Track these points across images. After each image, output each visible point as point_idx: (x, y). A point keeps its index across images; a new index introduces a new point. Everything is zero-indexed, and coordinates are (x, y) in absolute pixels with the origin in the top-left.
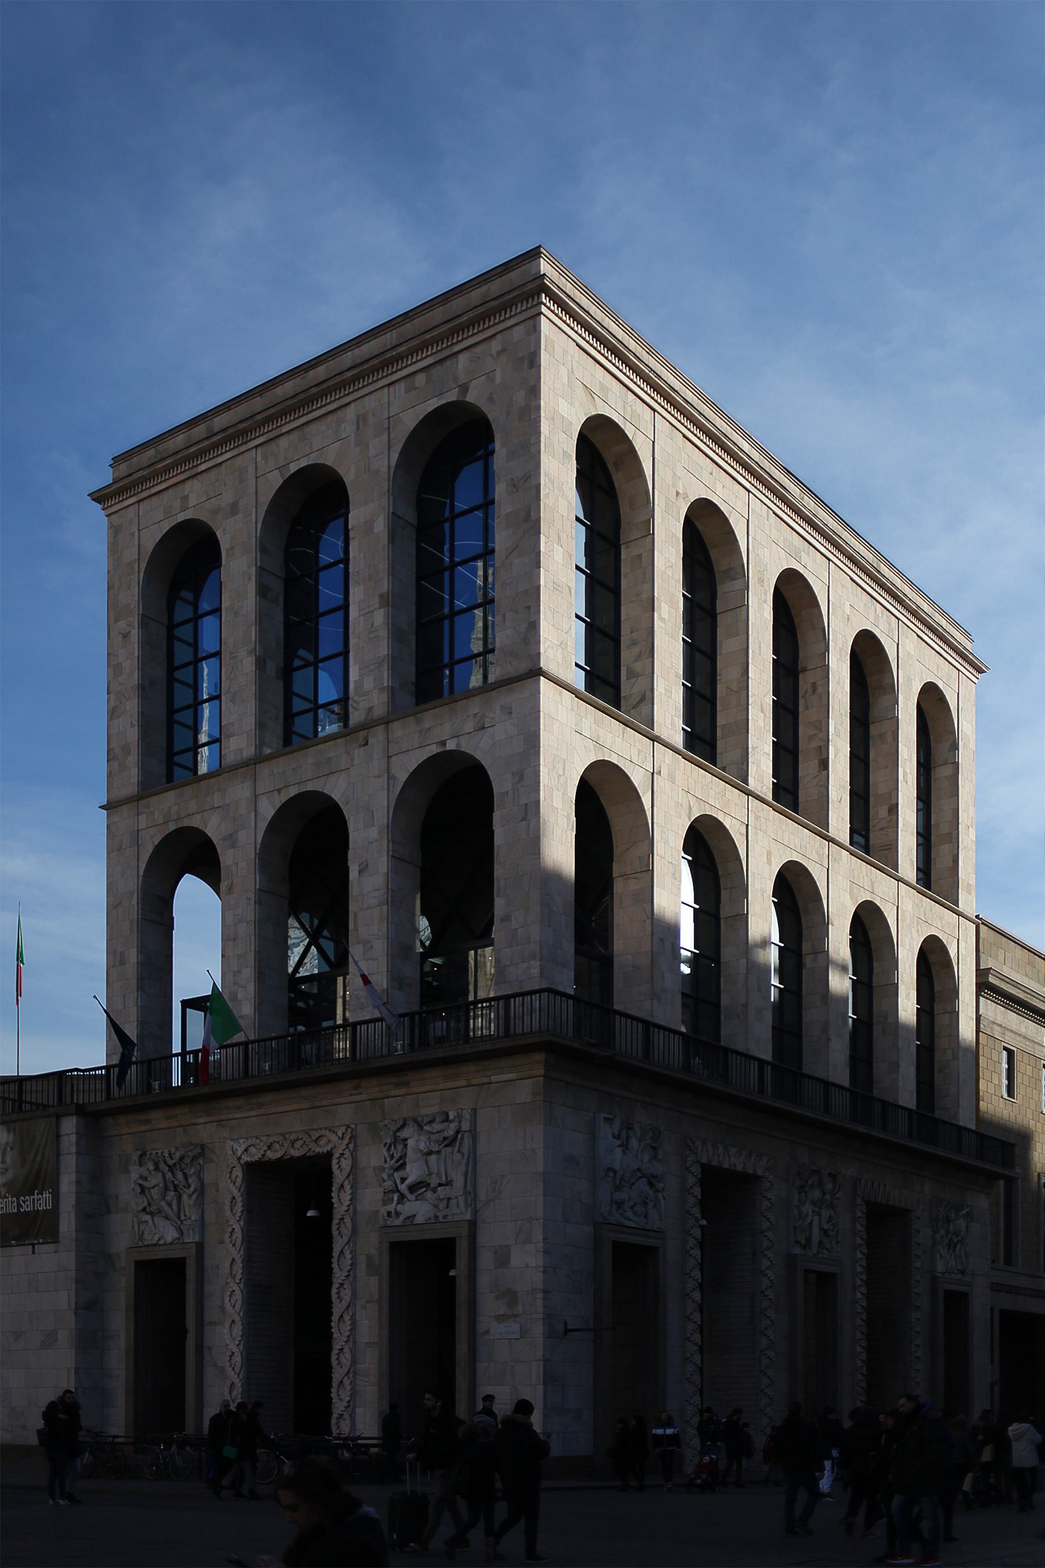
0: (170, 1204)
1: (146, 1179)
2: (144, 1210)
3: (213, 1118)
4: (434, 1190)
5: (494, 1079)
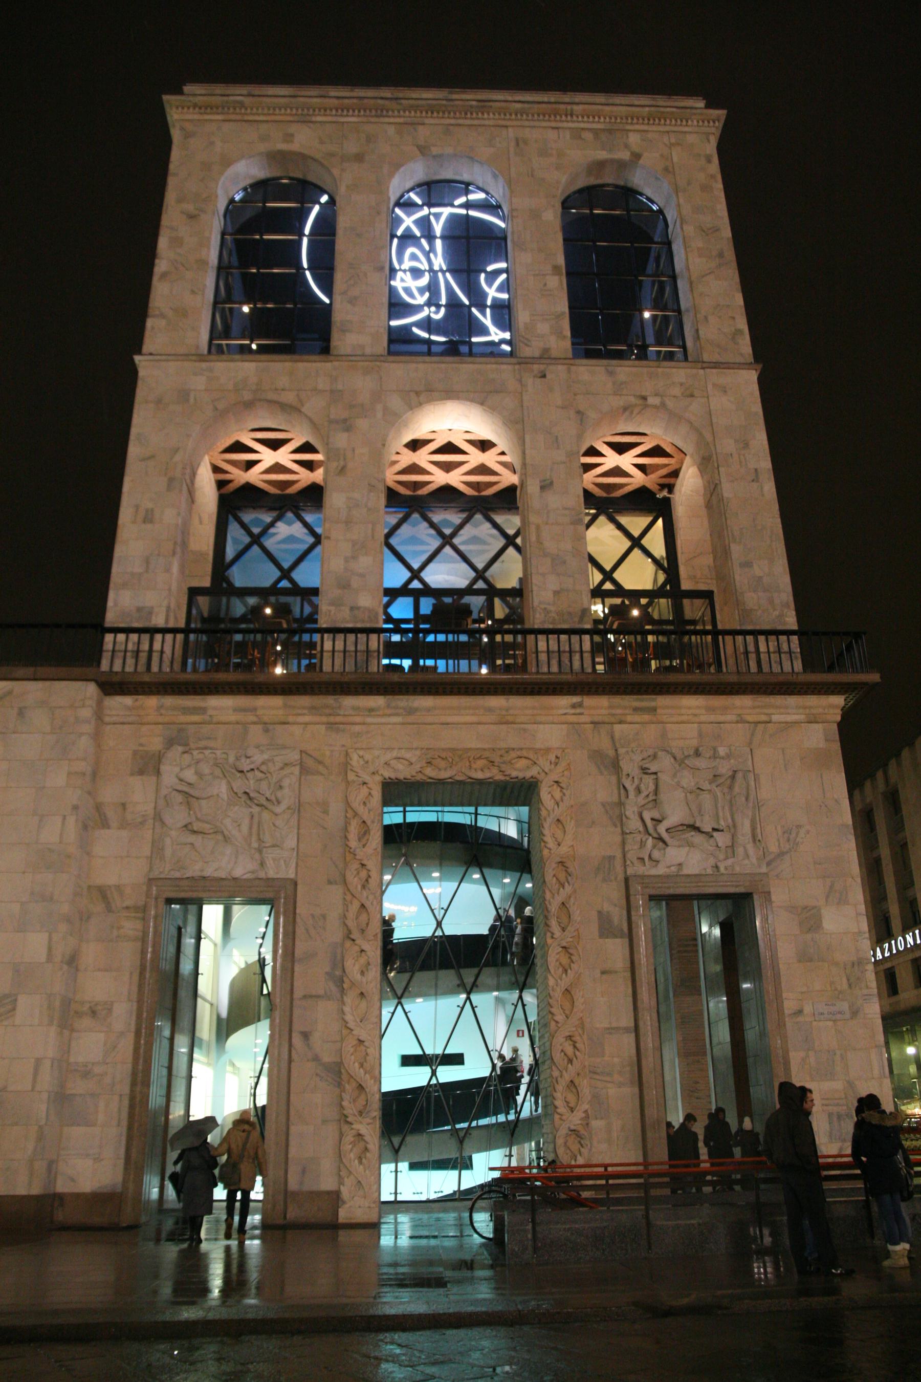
5: (775, 718)
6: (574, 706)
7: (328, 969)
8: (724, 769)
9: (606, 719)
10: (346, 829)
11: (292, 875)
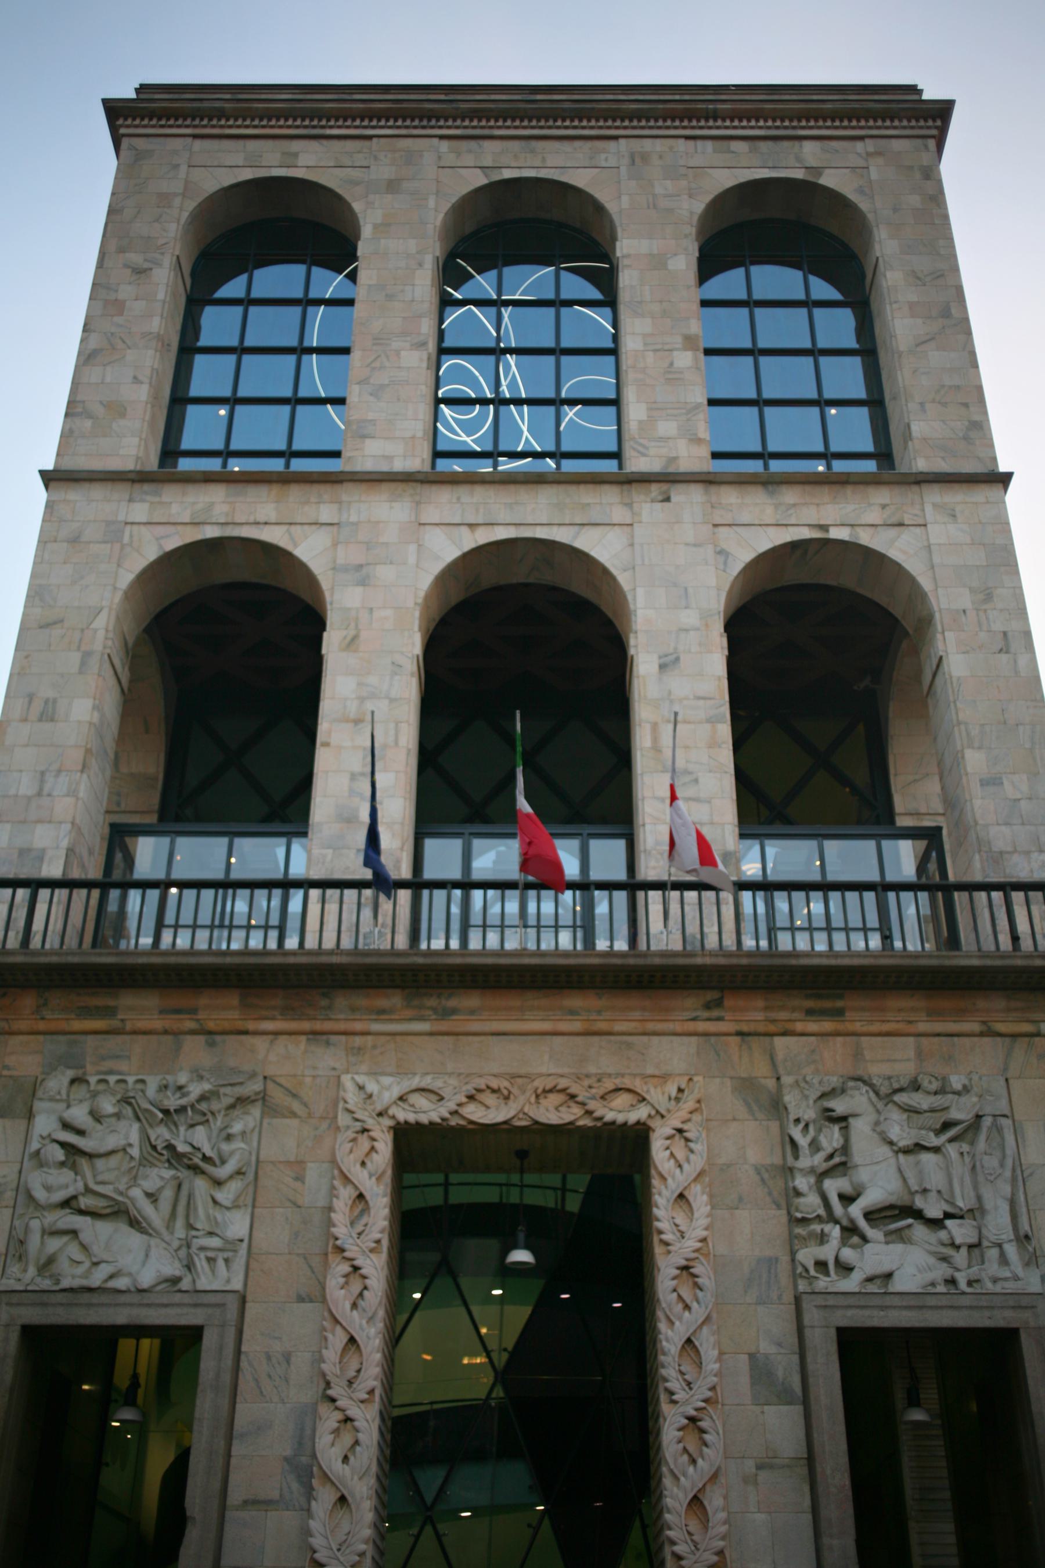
0: (152, 1197)
1: (81, 1133)
2: (66, 1203)
3: (306, 1025)
4: (936, 1224)
6: (708, 1006)
7: (288, 1452)
8: (961, 1111)
9: (761, 1028)
10: (330, 1209)
11: (237, 1285)
